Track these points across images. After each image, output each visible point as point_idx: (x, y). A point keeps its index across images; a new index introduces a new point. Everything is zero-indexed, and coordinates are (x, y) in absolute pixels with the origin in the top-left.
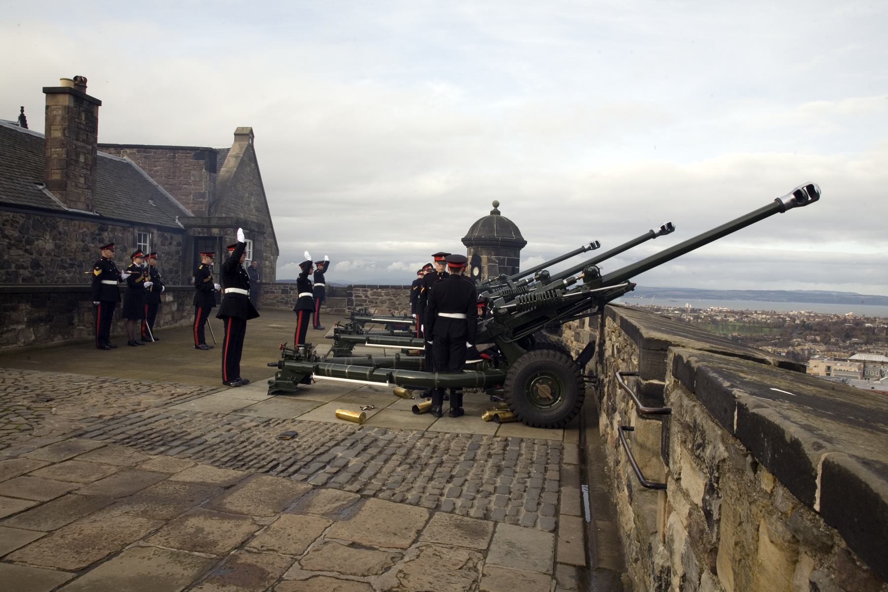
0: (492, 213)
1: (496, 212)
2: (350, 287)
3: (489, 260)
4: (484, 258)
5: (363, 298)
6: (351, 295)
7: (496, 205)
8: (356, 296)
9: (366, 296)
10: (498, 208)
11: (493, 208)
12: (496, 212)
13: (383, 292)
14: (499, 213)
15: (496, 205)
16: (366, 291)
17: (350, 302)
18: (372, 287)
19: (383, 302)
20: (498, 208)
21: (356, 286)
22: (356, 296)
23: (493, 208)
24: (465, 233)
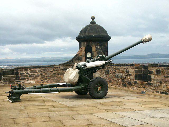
0: (92, 23)
1: (93, 22)
2: (17, 69)
3: (96, 48)
4: (94, 49)
5: (26, 74)
6: (17, 73)
7: (93, 18)
8: (21, 74)
9: (27, 73)
10: (95, 20)
11: (92, 20)
12: (93, 22)
13: (37, 70)
14: (95, 23)
15: (93, 18)
16: (27, 70)
17: (17, 78)
18: (30, 68)
19: (38, 76)
20: (95, 20)
21: (20, 68)
22: (21, 74)
23: (92, 20)
24: (77, 34)
